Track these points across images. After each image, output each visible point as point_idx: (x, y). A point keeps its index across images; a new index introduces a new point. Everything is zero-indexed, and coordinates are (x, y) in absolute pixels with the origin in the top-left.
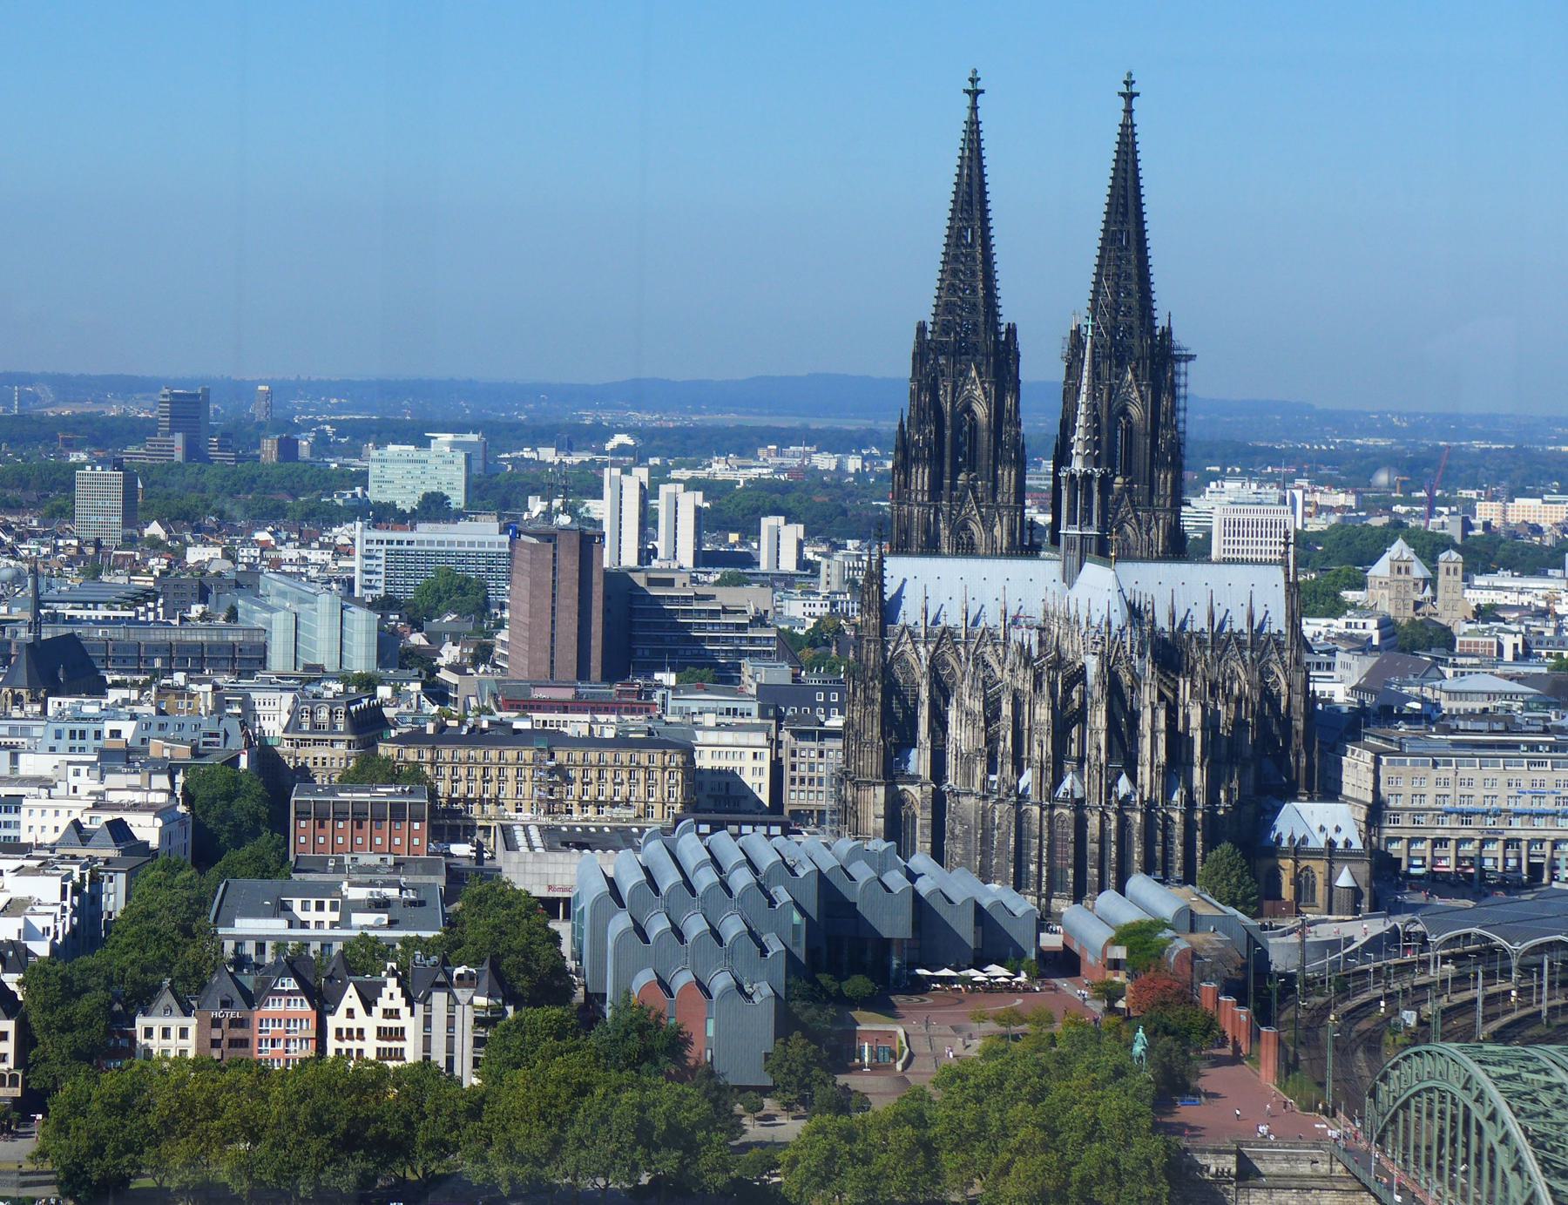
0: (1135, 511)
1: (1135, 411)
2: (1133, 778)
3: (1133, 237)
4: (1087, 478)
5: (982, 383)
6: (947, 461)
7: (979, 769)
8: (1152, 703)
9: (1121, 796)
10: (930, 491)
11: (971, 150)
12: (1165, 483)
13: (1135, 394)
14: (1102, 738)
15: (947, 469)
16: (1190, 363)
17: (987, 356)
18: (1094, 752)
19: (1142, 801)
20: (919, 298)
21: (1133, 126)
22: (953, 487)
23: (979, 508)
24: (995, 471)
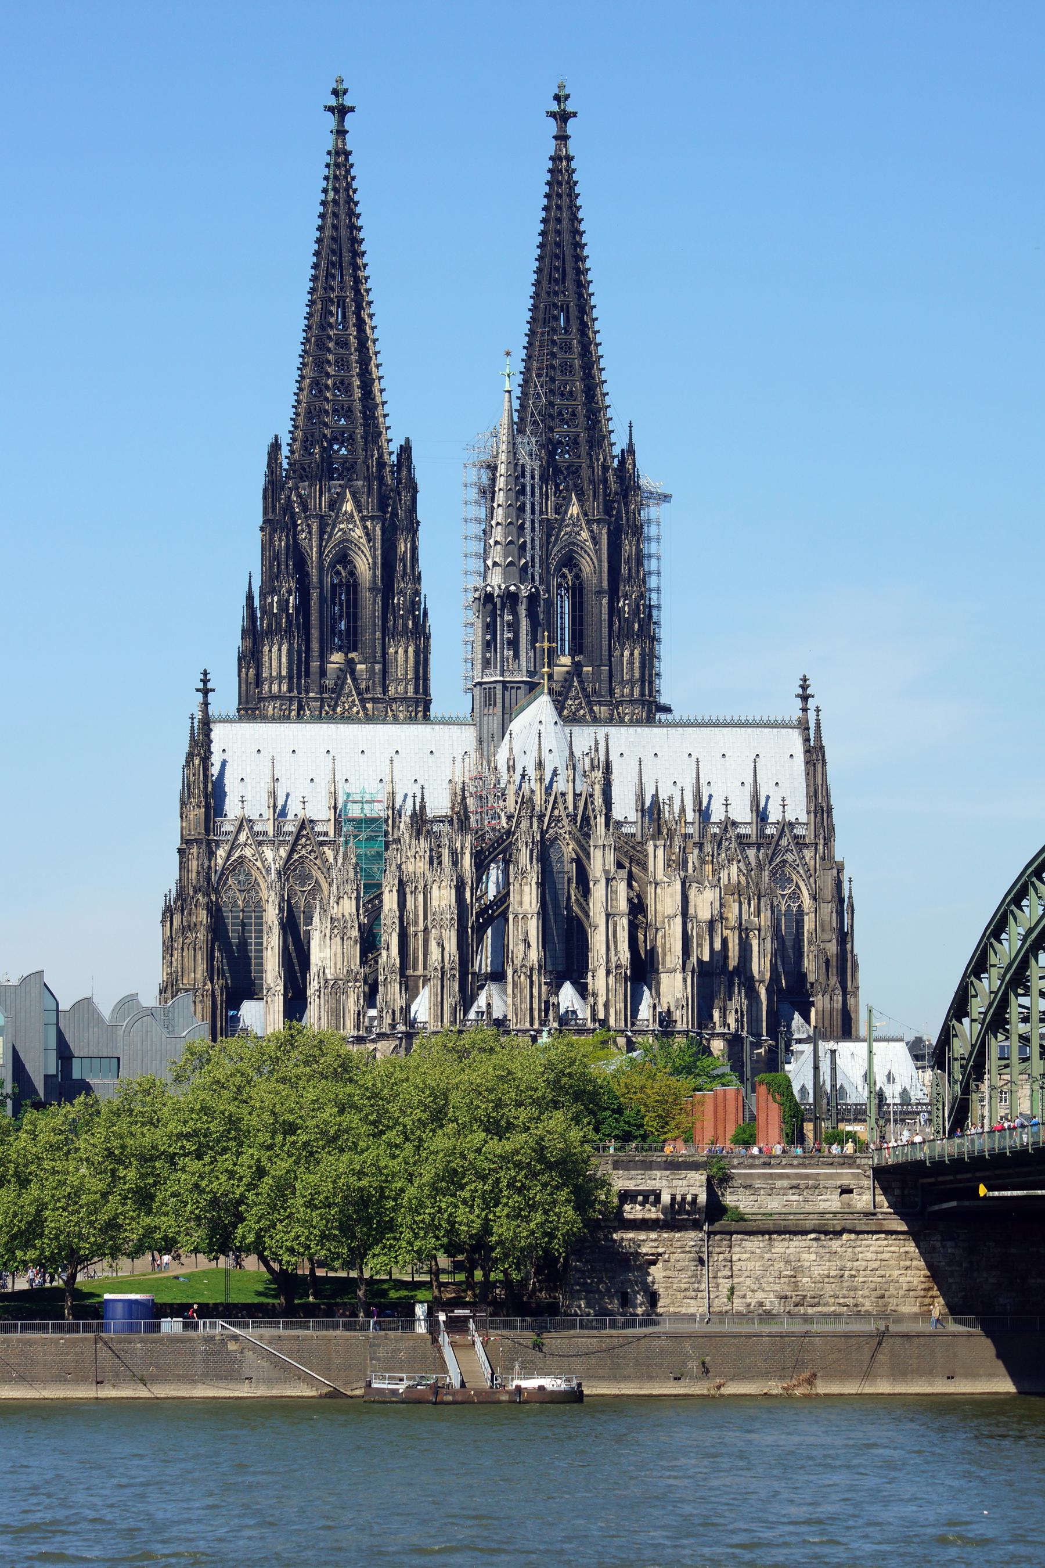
0: (589, 703)
1: (587, 566)
2: (583, 991)
3: (574, 312)
4: (511, 598)
5: (363, 519)
6: (315, 633)
7: (352, 1002)
8: (606, 872)
9: (562, 1011)
10: (290, 677)
11: (336, 190)
12: (631, 663)
13: (585, 535)
14: (533, 927)
15: (315, 645)
16: (665, 506)
17: (368, 479)
18: (521, 947)
19: (594, 1019)
20: (268, 407)
21: (569, 159)
22: (323, 672)
23: (363, 701)
24: (384, 653)
